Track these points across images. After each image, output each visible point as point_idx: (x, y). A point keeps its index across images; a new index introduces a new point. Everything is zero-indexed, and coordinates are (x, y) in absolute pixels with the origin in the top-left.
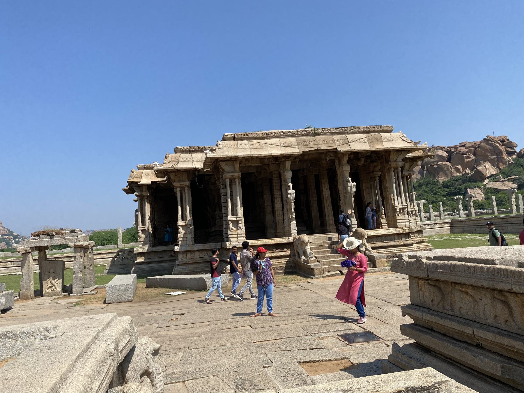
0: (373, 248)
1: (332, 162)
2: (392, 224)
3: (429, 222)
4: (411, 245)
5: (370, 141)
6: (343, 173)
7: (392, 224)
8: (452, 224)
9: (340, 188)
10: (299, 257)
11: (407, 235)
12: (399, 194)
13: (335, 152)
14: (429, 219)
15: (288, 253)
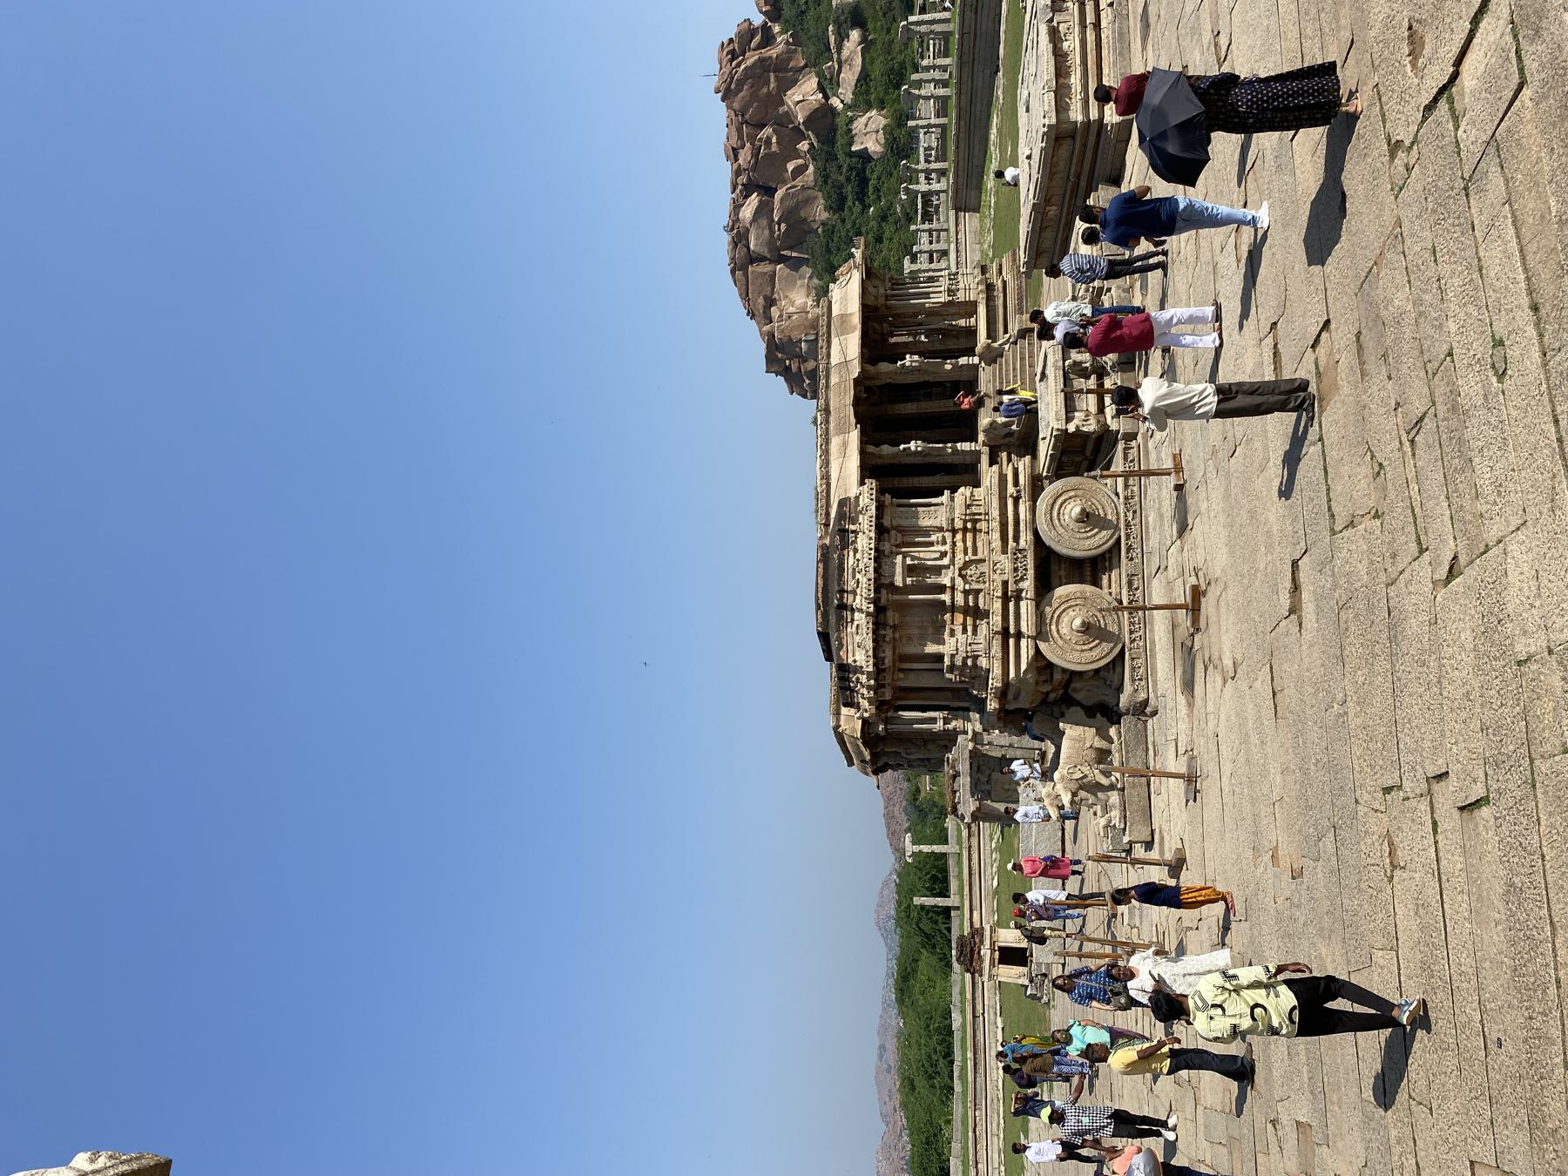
0: (1006, 332)
1: (868, 390)
2: (970, 309)
3: (953, 255)
4: (1004, 282)
5: (845, 330)
6: (889, 374)
7: (970, 309)
8: (959, 208)
9: (910, 379)
10: (1011, 434)
11: (990, 288)
12: (927, 295)
13: (857, 382)
14: (945, 253)
15: (1004, 455)
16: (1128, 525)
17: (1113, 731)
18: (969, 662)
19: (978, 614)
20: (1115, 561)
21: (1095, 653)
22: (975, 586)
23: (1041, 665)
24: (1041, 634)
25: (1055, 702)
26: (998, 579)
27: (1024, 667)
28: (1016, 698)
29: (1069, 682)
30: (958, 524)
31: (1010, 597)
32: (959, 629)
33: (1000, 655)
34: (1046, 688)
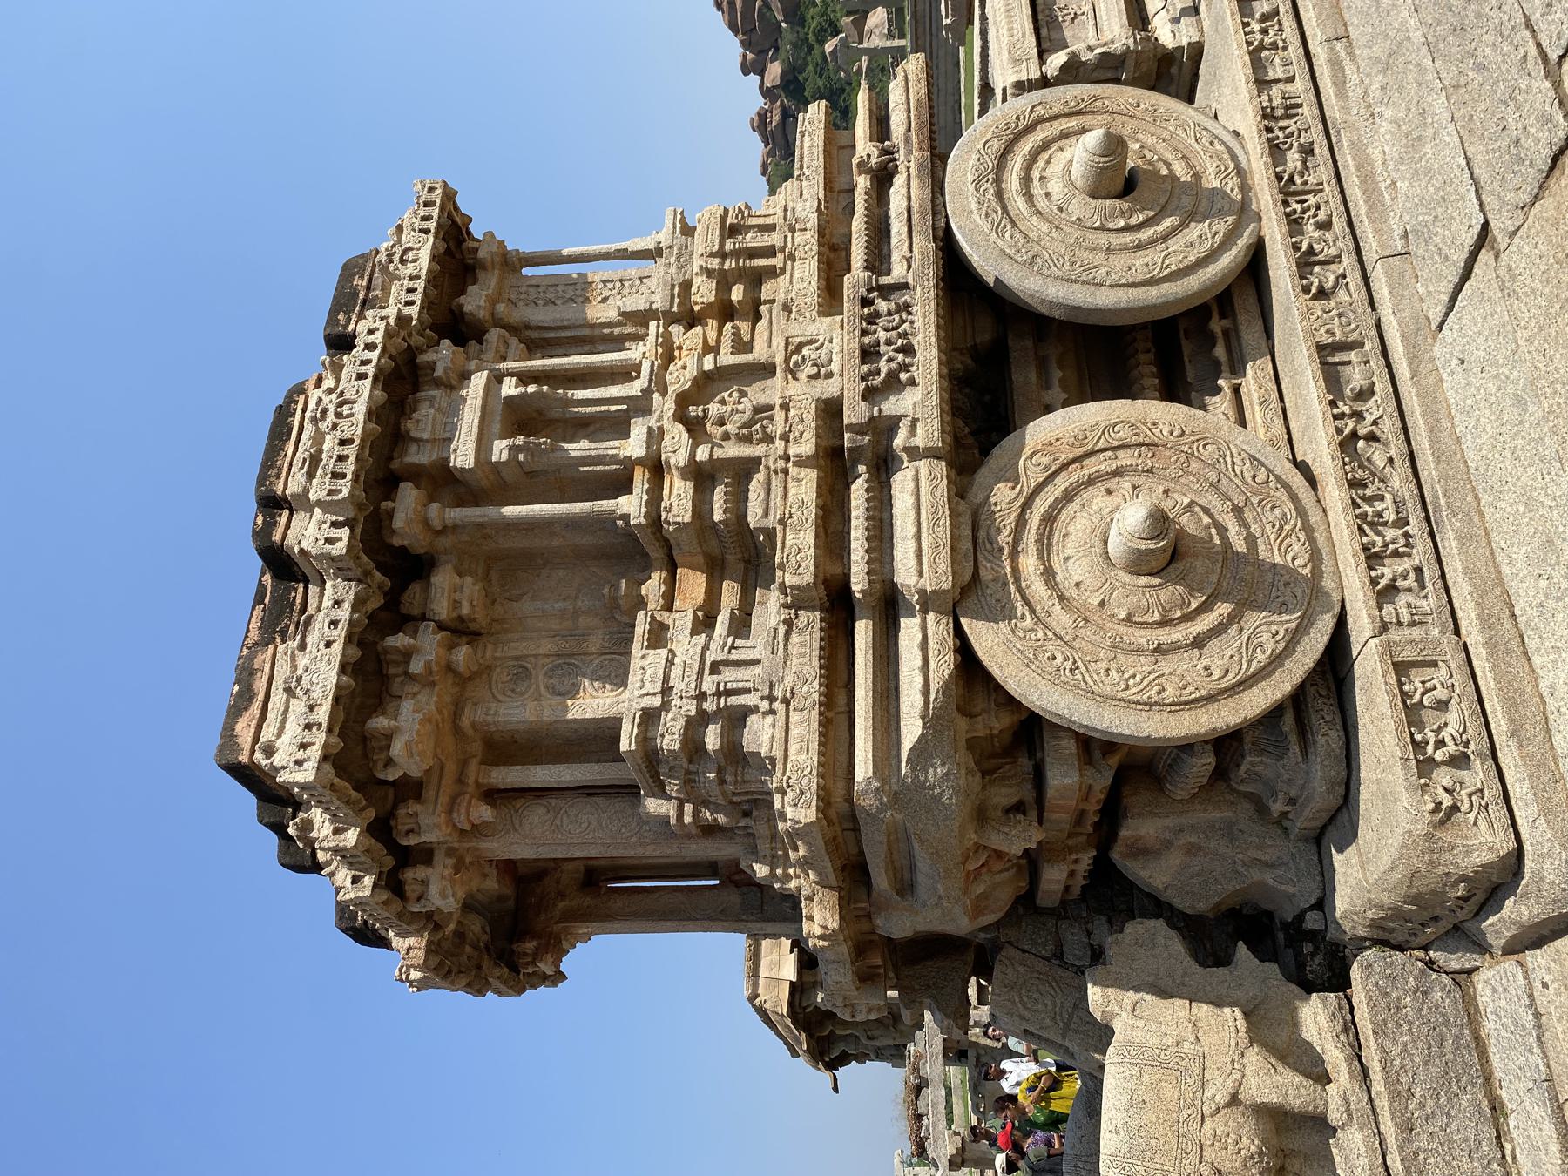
16: (1287, 189)
17: (1315, 1018)
18: (712, 738)
19: (742, 556)
20: (1250, 334)
21: (1223, 659)
22: (732, 450)
23: (1001, 735)
24: (974, 589)
25: (1063, 910)
26: (804, 394)
27: (911, 731)
28: (906, 887)
29: (1112, 813)
30: (704, 292)
31: (851, 457)
32: (681, 622)
33: (812, 690)
34: (1017, 839)
